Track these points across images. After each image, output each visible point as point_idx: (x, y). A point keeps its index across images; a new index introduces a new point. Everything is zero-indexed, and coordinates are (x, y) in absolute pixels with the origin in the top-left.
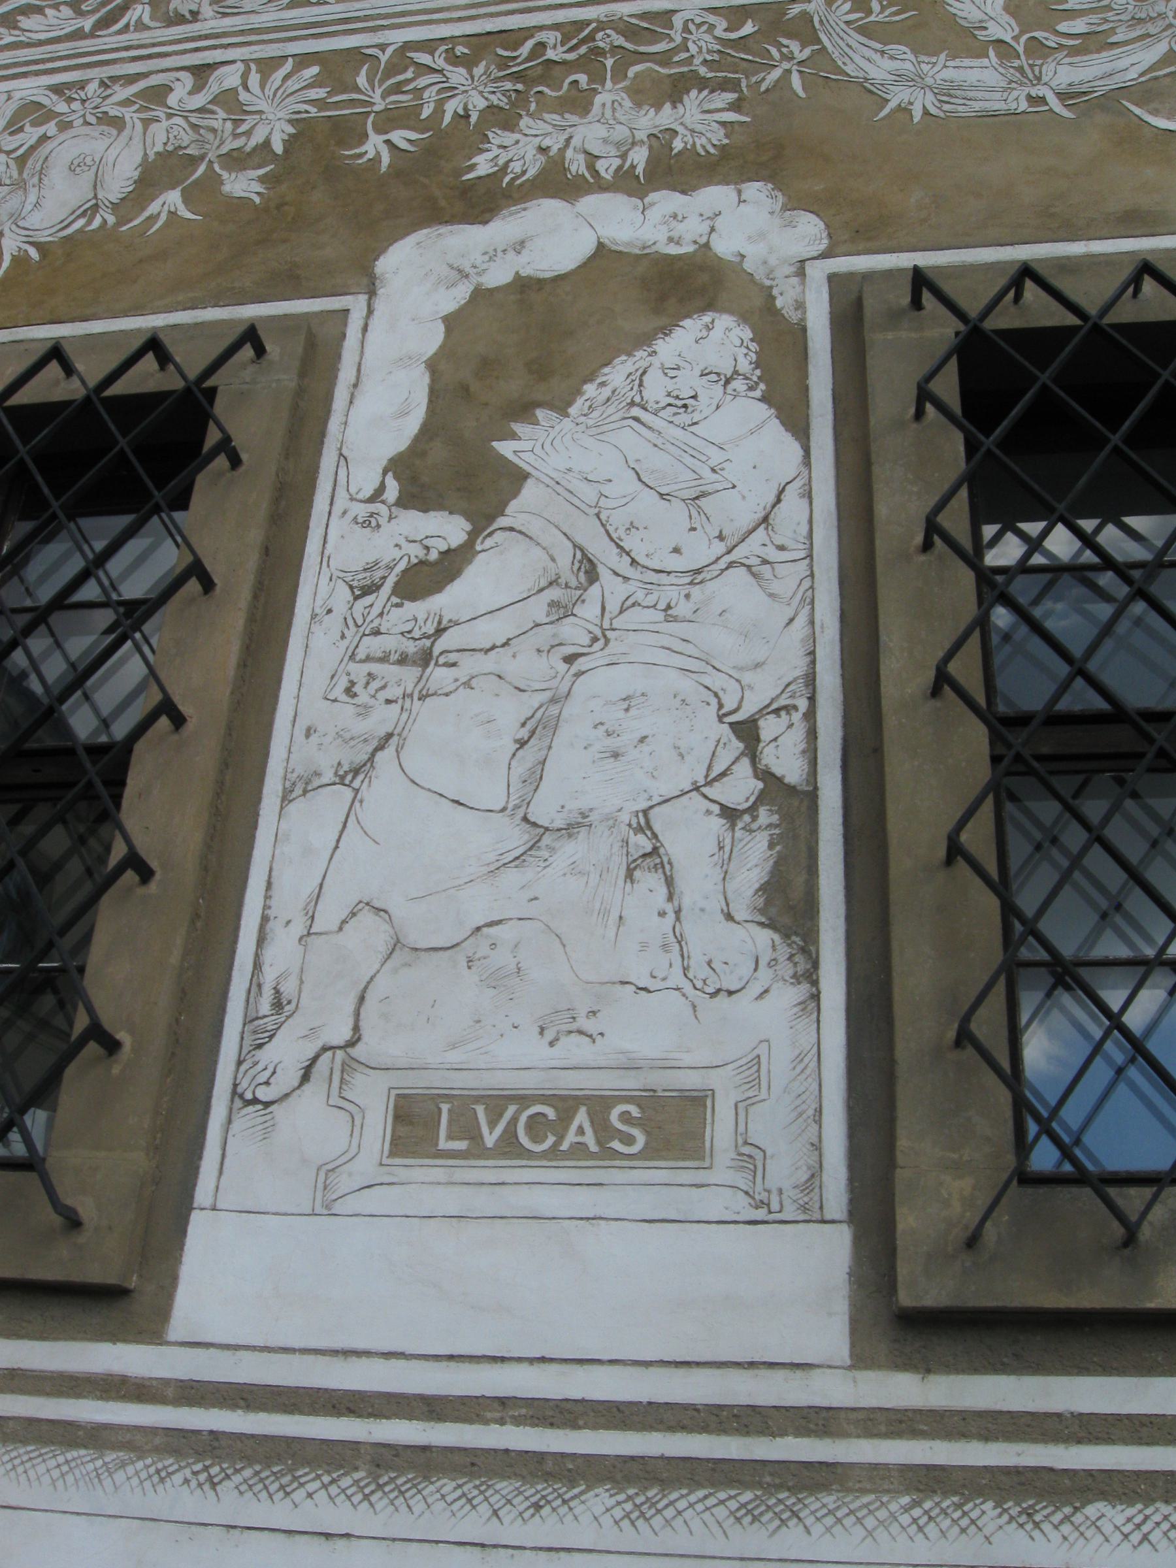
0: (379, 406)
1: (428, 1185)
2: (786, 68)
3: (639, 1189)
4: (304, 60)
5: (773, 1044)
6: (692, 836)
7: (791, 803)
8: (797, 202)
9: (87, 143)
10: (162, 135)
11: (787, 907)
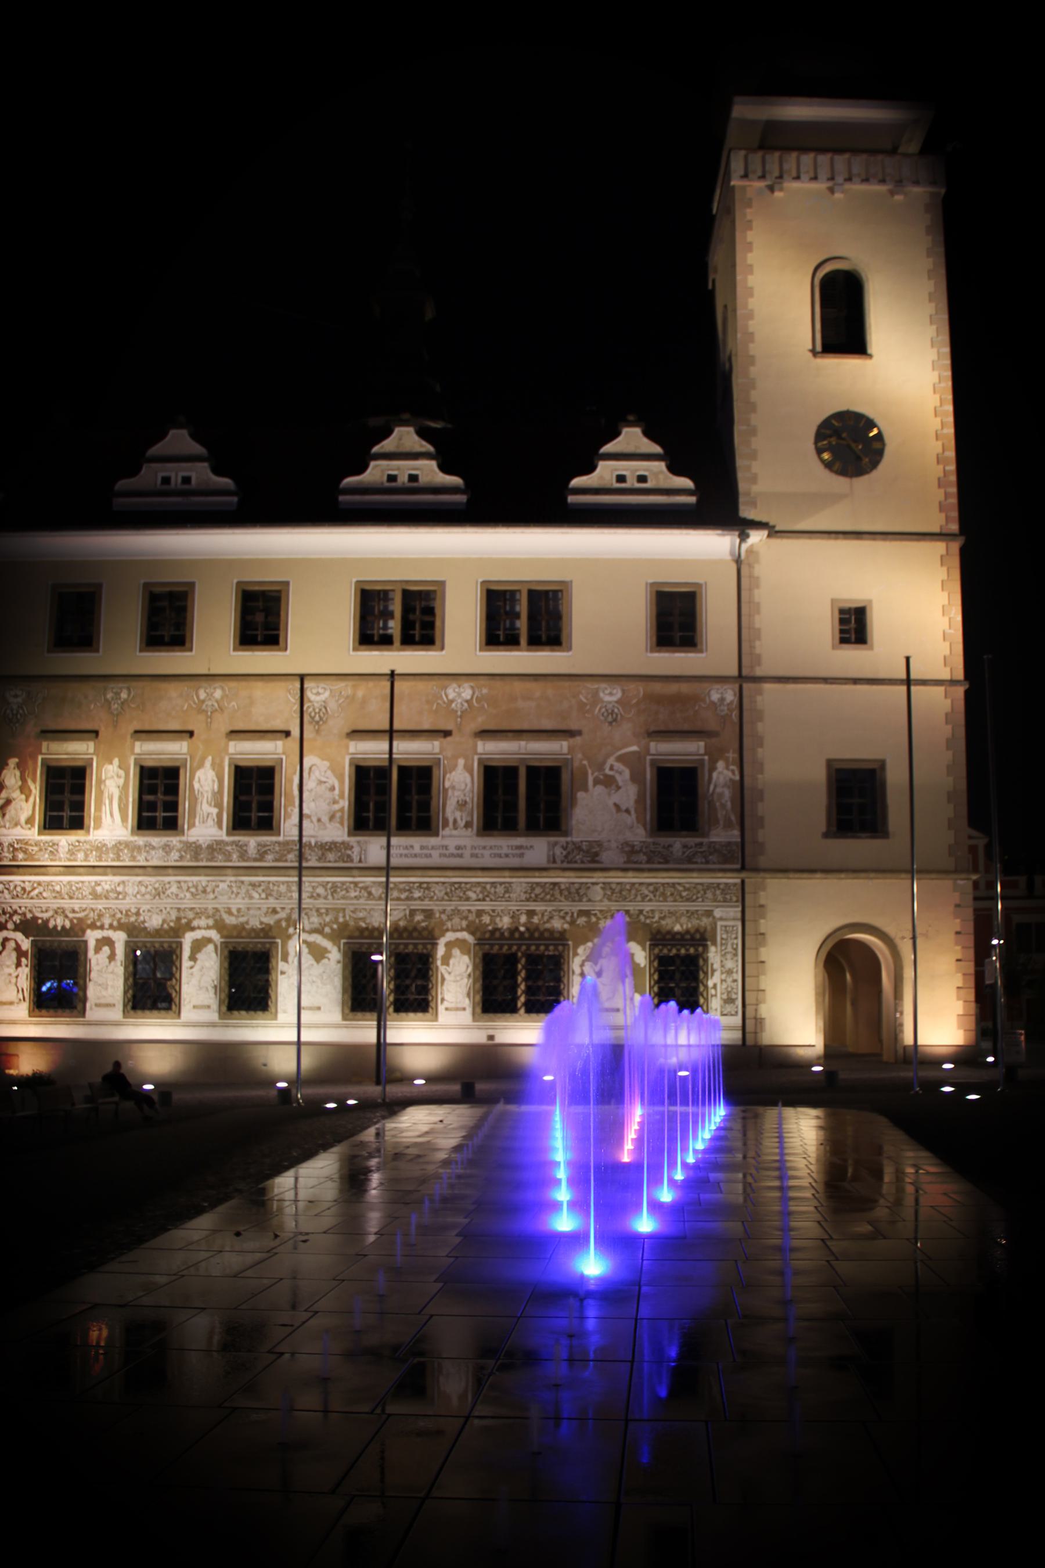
2: (217, 917)
3: (206, 1010)
7: (216, 987)
9: (155, 917)
10: (164, 916)
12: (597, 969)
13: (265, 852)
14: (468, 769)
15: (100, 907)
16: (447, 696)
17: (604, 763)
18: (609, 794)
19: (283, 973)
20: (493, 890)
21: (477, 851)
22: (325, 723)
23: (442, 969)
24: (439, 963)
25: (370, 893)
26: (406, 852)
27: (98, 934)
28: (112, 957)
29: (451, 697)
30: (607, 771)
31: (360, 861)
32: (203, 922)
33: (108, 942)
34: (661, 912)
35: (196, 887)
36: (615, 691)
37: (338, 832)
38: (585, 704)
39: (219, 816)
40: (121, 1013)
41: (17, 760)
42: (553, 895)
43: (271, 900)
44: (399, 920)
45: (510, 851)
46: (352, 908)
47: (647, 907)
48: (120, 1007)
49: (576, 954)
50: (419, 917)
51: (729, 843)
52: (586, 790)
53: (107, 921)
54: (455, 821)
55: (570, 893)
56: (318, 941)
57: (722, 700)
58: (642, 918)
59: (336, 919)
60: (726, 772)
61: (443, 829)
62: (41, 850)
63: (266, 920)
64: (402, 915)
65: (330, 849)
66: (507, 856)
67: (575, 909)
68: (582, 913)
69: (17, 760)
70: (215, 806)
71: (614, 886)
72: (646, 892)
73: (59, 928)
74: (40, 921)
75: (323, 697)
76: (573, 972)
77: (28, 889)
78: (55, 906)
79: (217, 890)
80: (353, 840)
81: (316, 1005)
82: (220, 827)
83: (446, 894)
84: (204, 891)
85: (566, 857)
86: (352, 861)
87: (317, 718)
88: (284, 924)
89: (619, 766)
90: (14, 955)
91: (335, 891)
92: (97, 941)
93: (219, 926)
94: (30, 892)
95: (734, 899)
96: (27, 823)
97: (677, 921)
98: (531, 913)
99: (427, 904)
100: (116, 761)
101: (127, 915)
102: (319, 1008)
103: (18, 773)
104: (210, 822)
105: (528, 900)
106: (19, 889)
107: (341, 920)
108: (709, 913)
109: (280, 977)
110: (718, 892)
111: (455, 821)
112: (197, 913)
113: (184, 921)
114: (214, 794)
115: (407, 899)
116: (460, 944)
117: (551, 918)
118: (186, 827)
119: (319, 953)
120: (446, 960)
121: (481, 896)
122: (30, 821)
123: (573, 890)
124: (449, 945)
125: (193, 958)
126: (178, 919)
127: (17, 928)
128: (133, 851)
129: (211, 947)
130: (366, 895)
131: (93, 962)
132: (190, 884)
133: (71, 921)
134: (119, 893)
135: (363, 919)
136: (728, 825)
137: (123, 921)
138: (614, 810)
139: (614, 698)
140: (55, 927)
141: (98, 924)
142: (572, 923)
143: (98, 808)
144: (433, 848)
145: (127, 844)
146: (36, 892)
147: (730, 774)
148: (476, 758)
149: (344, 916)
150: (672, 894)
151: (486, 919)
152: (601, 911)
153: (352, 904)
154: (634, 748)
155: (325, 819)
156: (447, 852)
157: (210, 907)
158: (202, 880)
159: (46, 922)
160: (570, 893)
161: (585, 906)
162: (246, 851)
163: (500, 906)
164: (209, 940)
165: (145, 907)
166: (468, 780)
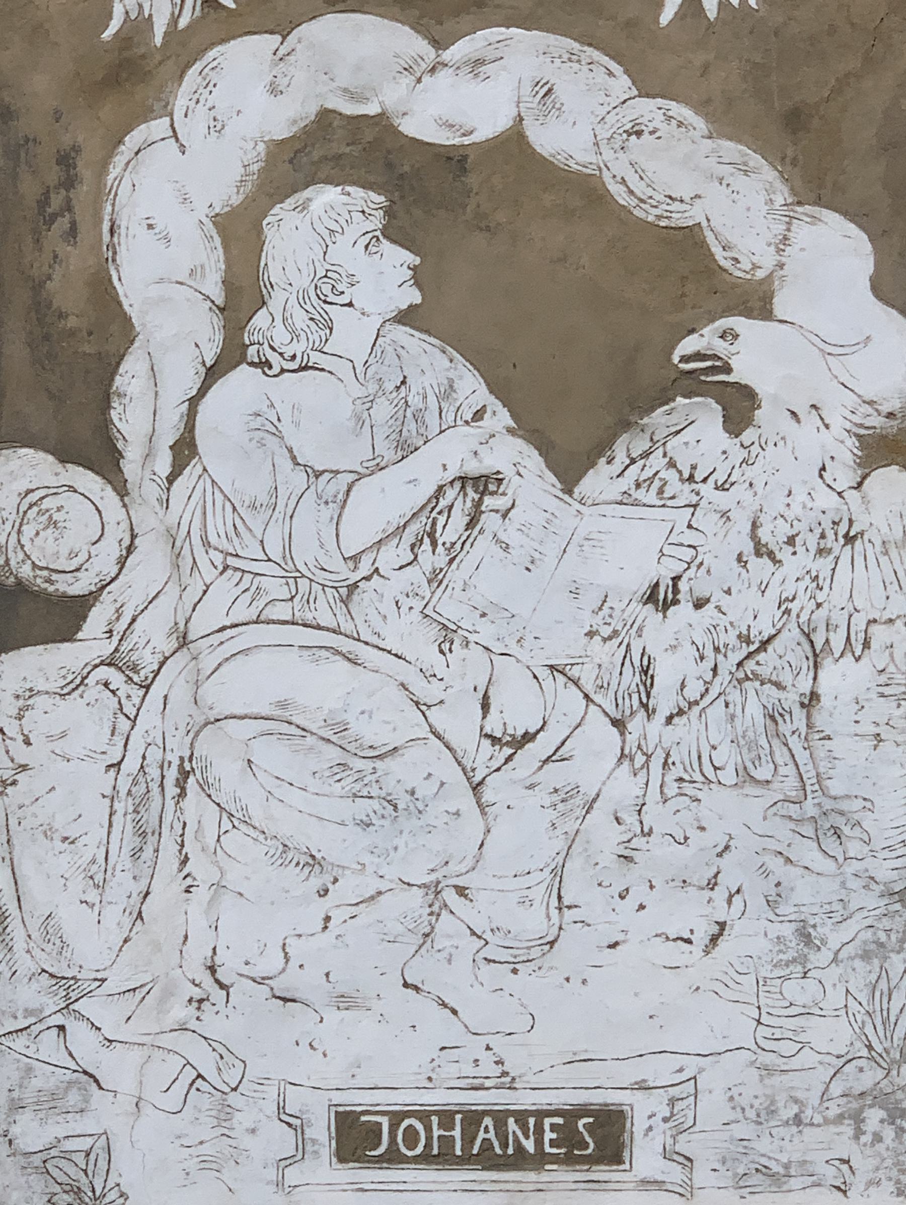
56: (555, 140)
81: (548, 1081)
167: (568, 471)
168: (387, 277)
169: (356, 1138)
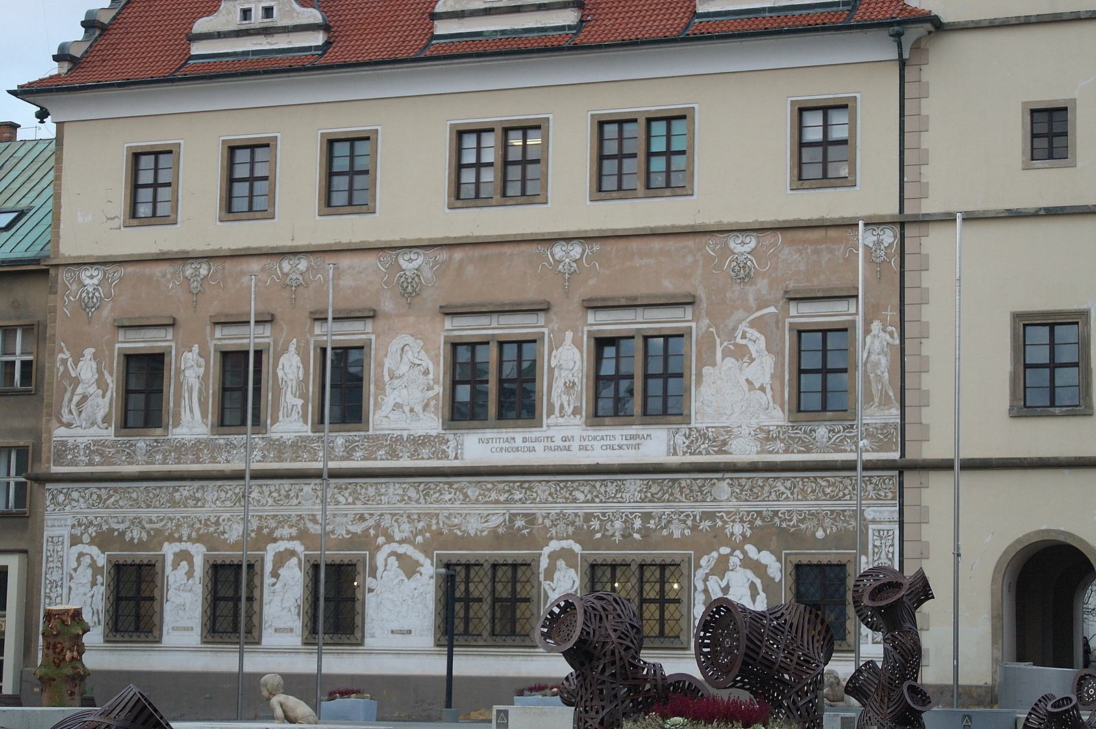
0: (268, 567)
1: (277, 634)
2: (301, 525)
3: (289, 634)
4: (257, 516)
5: (298, 624)
6: (293, 609)
8: (302, 544)
9: (235, 526)
11: (299, 614)
12: (723, 584)
13: (353, 449)
14: (577, 343)
15: (178, 516)
16: (553, 256)
17: (735, 329)
18: (741, 369)
19: (371, 590)
20: (603, 489)
21: (586, 443)
22: (418, 295)
23: (546, 585)
24: (542, 577)
25: (466, 495)
26: (507, 445)
27: (177, 547)
28: (190, 574)
29: (557, 257)
30: (739, 340)
31: (456, 458)
32: (286, 531)
33: (184, 556)
34: (800, 513)
35: (279, 491)
36: (748, 240)
37: (431, 424)
38: (713, 258)
39: (305, 407)
40: (199, 638)
41: (94, 350)
42: (672, 494)
43: (359, 505)
44: (498, 526)
45: (625, 442)
46: (446, 513)
47: (783, 506)
48: (198, 630)
49: (698, 566)
50: (519, 523)
51: (886, 425)
52: (714, 364)
53: (185, 532)
54: (562, 407)
55: (692, 491)
56: (408, 553)
57: (879, 242)
58: (776, 520)
59: (429, 526)
60: (882, 334)
61: (549, 414)
62: (118, 452)
63: (353, 529)
64: (501, 519)
65: (423, 444)
66: (620, 447)
67: (698, 511)
68: (706, 516)
69: (93, 350)
70: (299, 397)
71: (743, 482)
72: (782, 489)
73: (136, 541)
74: (116, 533)
75: (415, 264)
76: (695, 589)
77: (104, 497)
78: (132, 516)
79: (300, 494)
80: (450, 436)
81: (406, 628)
82: (306, 422)
83: (550, 494)
84: (287, 497)
85: (688, 447)
86: (447, 457)
87: (410, 289)
88: (372, 532)
89: (753, 333)
90: (89, 572)
91: (427, 494)
92: (175, 554)
93: (303, 536)
94: (106, 500)
95: (890, 495)
96: (103, 422)
97: (820, 524)
98: (646, 517)
99: (529, 508)
100: (196, 348)
101: (206, 525)
102: (410, 632)
103: (95, 366)
104: (295, 416)
105: (643, 501)
106: (95, 497)
107: (434, 527)
108: (858, 514)
109: (368, 596)
110: (870, 488)
111: (562, 407)
112: (280, 522)
113: (266, 531)
114: (299, 383)
115: (507, 501)
116: (566, 554)
117: (670, 522)
118: (269, 421)
119: (410, 568)
120: (550, 574)
121: (589, 497)
122: (106, 419)
123: (695, 488)
124: (553, 556)
125: (275, 574)
126: (260, 529)
127: (92, 542)
128: (213, 451)
129: (294, 560)
130: (461, 497)
131: (171, 580)
132: (273, 488)
133: (148, 533)
134: (198, 500)
135: (458, 526)
136: (885, 402)
137: (201, 532)
138: (746, 387)
139: (747, 248)
140: (133, 539)
141: (176, 535)
142: (694, 528)
143: (178, 404)
144: (537, 440)
145: (207, 443)
146: (112, 500)
147: (888, 337)
148: (586, 329)
149: (438, 523)
150: (813, 491)
151: (595, 524)
152: (728, 513)
153: (447, 509)
154: (772, 309)
155: (418, 408)
156: (553, 444)
157: (293, 514)
158: (286, 484)
159: (122, 534)
160: (692, 491)
161: (708, 507)
162: (332, 448)
163: (611, 507)
164: (292, 553)
165: (226, 516)
166: (577, 356)
167: (409, 579)
168: (396, 564)
169: (392, 632)
